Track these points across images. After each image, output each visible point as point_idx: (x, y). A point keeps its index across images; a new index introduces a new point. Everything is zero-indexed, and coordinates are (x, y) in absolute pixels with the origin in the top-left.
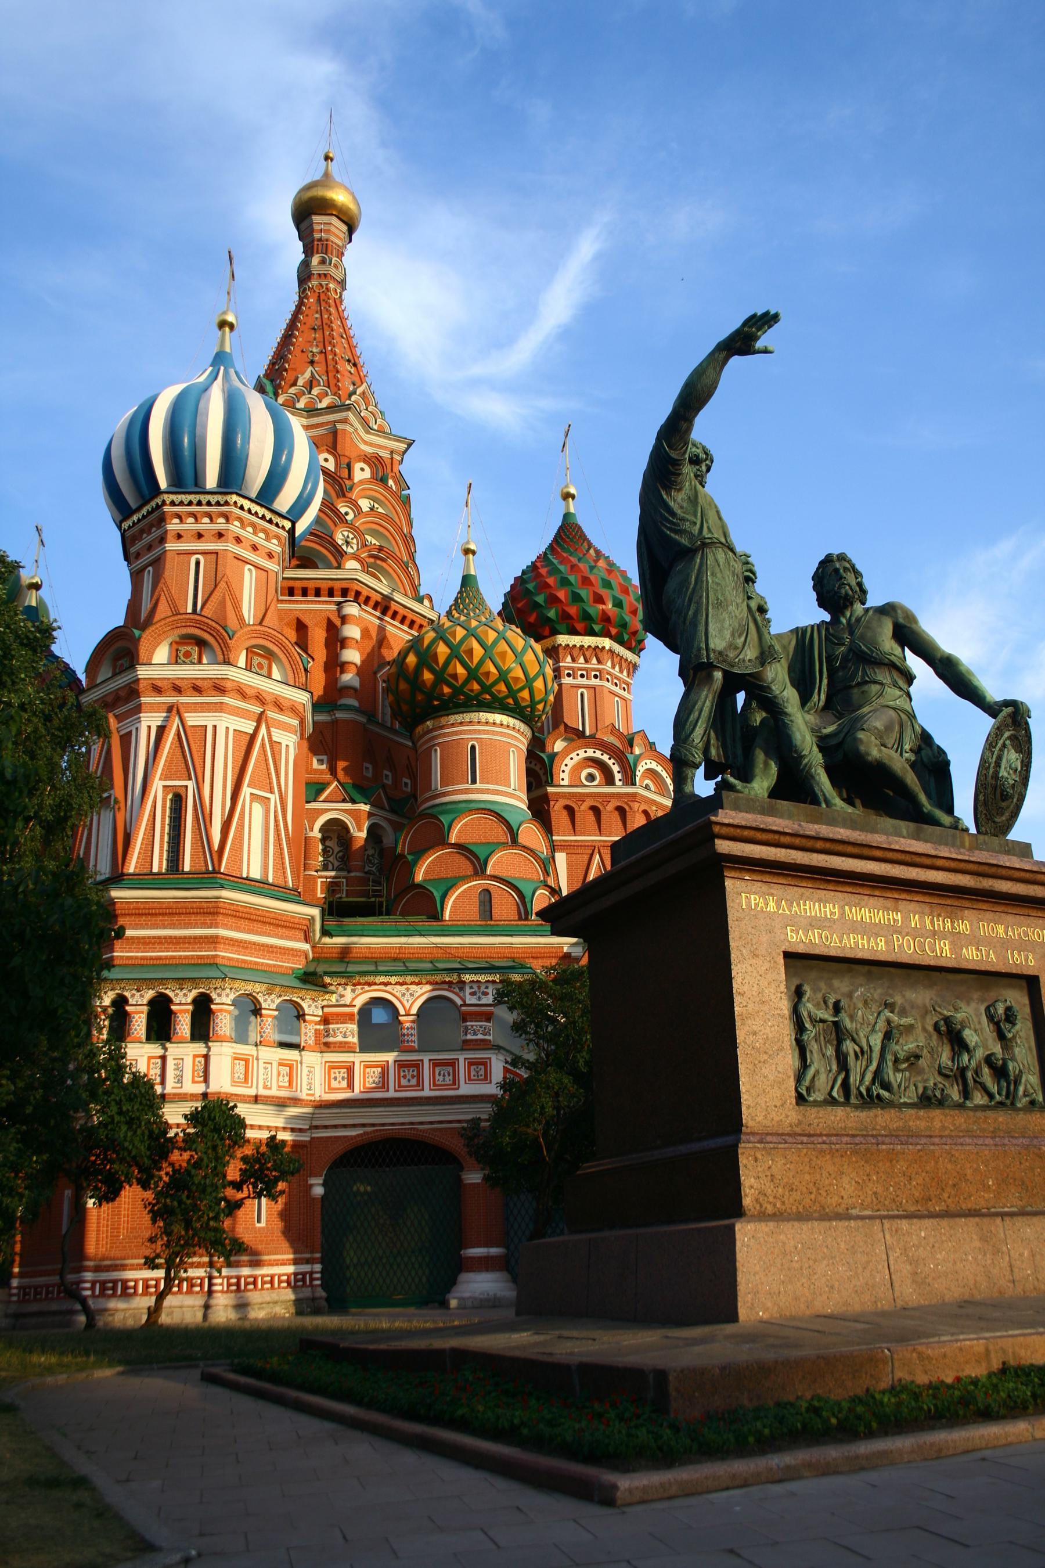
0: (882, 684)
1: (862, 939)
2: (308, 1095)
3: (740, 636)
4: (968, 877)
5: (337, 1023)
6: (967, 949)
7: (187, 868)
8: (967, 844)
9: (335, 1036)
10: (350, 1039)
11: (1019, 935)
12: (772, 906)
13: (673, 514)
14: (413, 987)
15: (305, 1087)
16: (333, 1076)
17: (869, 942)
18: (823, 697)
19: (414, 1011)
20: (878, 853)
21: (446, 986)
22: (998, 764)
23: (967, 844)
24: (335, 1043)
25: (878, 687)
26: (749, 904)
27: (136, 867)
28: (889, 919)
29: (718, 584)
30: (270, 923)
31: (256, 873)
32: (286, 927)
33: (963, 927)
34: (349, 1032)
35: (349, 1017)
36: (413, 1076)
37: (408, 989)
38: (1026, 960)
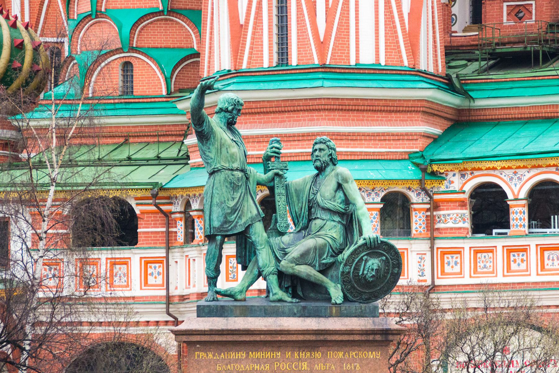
0: (324, 220)
1: (257, 365)
2: (419, 281)
3: (234, 213)
4: (312, 336)
5: (447, 209)
6: (318, 365)
7: (294, 61)
8: (334, 311)
9: (445, 222)
10: (461, 225)
11: (353, 356)
12: (210, 355)
13: (205, 154)
14: (520, 172)
15: (523, 229)
16: (446, 261)
17: (260, 367)
18: (305, 221)
19: (523, 194)
20: (258, 332)
21: (554, 169)
22: (357, 269)
23: (334, 311)
24: (447, 229)
25: (321, 221)
26: (198, 356)
27: (249, 63)
28: (273, 356)
29: (218, 194)
30: (381, 111)
31: (367, 58)
32: (399, 111)
33: (318, 355)
34: (458, 218)
35: (462, 204)
36: (522, 261)
37: (515, 173)
38: (355, 367)
